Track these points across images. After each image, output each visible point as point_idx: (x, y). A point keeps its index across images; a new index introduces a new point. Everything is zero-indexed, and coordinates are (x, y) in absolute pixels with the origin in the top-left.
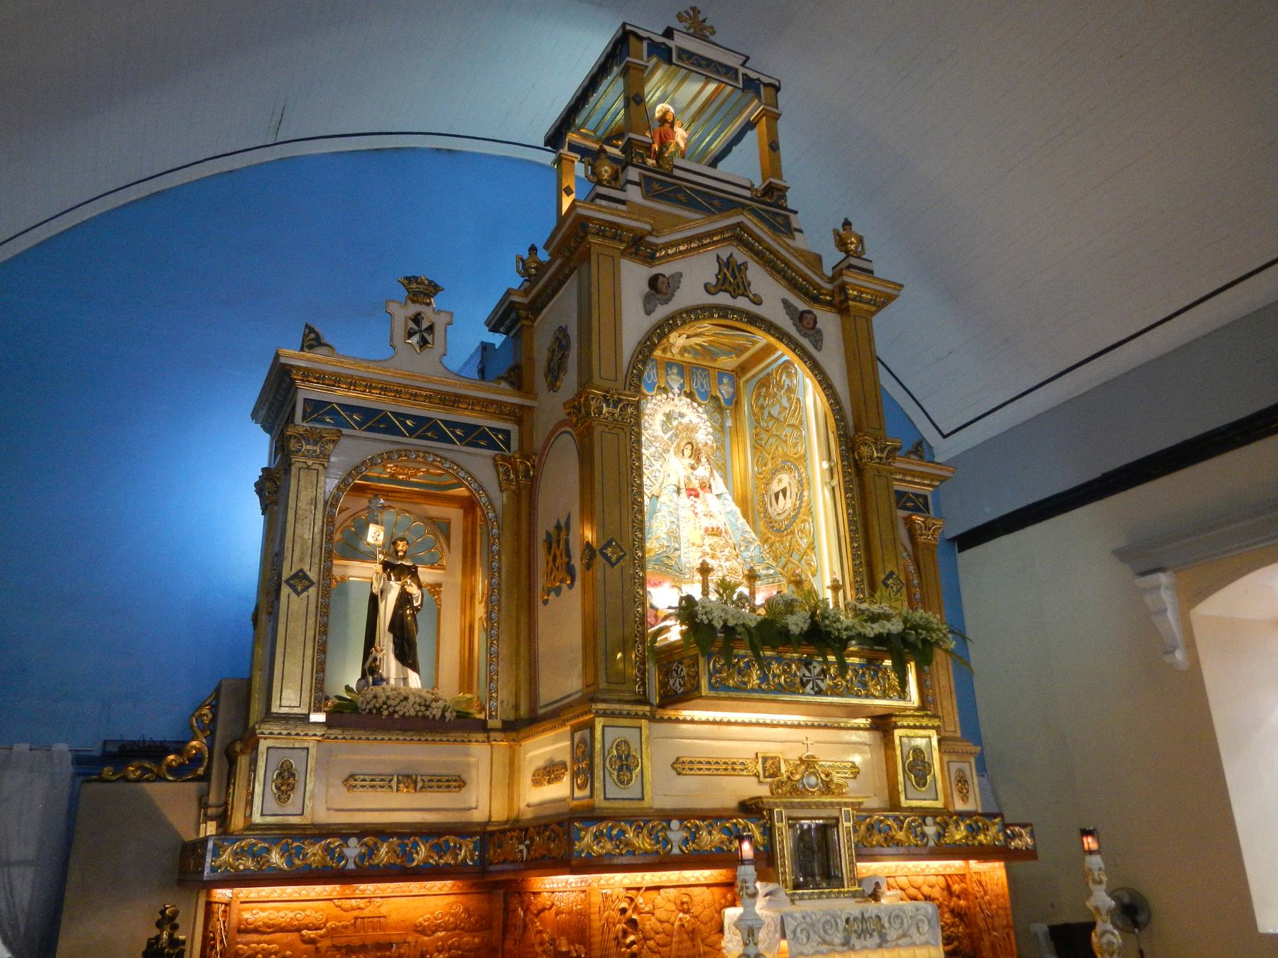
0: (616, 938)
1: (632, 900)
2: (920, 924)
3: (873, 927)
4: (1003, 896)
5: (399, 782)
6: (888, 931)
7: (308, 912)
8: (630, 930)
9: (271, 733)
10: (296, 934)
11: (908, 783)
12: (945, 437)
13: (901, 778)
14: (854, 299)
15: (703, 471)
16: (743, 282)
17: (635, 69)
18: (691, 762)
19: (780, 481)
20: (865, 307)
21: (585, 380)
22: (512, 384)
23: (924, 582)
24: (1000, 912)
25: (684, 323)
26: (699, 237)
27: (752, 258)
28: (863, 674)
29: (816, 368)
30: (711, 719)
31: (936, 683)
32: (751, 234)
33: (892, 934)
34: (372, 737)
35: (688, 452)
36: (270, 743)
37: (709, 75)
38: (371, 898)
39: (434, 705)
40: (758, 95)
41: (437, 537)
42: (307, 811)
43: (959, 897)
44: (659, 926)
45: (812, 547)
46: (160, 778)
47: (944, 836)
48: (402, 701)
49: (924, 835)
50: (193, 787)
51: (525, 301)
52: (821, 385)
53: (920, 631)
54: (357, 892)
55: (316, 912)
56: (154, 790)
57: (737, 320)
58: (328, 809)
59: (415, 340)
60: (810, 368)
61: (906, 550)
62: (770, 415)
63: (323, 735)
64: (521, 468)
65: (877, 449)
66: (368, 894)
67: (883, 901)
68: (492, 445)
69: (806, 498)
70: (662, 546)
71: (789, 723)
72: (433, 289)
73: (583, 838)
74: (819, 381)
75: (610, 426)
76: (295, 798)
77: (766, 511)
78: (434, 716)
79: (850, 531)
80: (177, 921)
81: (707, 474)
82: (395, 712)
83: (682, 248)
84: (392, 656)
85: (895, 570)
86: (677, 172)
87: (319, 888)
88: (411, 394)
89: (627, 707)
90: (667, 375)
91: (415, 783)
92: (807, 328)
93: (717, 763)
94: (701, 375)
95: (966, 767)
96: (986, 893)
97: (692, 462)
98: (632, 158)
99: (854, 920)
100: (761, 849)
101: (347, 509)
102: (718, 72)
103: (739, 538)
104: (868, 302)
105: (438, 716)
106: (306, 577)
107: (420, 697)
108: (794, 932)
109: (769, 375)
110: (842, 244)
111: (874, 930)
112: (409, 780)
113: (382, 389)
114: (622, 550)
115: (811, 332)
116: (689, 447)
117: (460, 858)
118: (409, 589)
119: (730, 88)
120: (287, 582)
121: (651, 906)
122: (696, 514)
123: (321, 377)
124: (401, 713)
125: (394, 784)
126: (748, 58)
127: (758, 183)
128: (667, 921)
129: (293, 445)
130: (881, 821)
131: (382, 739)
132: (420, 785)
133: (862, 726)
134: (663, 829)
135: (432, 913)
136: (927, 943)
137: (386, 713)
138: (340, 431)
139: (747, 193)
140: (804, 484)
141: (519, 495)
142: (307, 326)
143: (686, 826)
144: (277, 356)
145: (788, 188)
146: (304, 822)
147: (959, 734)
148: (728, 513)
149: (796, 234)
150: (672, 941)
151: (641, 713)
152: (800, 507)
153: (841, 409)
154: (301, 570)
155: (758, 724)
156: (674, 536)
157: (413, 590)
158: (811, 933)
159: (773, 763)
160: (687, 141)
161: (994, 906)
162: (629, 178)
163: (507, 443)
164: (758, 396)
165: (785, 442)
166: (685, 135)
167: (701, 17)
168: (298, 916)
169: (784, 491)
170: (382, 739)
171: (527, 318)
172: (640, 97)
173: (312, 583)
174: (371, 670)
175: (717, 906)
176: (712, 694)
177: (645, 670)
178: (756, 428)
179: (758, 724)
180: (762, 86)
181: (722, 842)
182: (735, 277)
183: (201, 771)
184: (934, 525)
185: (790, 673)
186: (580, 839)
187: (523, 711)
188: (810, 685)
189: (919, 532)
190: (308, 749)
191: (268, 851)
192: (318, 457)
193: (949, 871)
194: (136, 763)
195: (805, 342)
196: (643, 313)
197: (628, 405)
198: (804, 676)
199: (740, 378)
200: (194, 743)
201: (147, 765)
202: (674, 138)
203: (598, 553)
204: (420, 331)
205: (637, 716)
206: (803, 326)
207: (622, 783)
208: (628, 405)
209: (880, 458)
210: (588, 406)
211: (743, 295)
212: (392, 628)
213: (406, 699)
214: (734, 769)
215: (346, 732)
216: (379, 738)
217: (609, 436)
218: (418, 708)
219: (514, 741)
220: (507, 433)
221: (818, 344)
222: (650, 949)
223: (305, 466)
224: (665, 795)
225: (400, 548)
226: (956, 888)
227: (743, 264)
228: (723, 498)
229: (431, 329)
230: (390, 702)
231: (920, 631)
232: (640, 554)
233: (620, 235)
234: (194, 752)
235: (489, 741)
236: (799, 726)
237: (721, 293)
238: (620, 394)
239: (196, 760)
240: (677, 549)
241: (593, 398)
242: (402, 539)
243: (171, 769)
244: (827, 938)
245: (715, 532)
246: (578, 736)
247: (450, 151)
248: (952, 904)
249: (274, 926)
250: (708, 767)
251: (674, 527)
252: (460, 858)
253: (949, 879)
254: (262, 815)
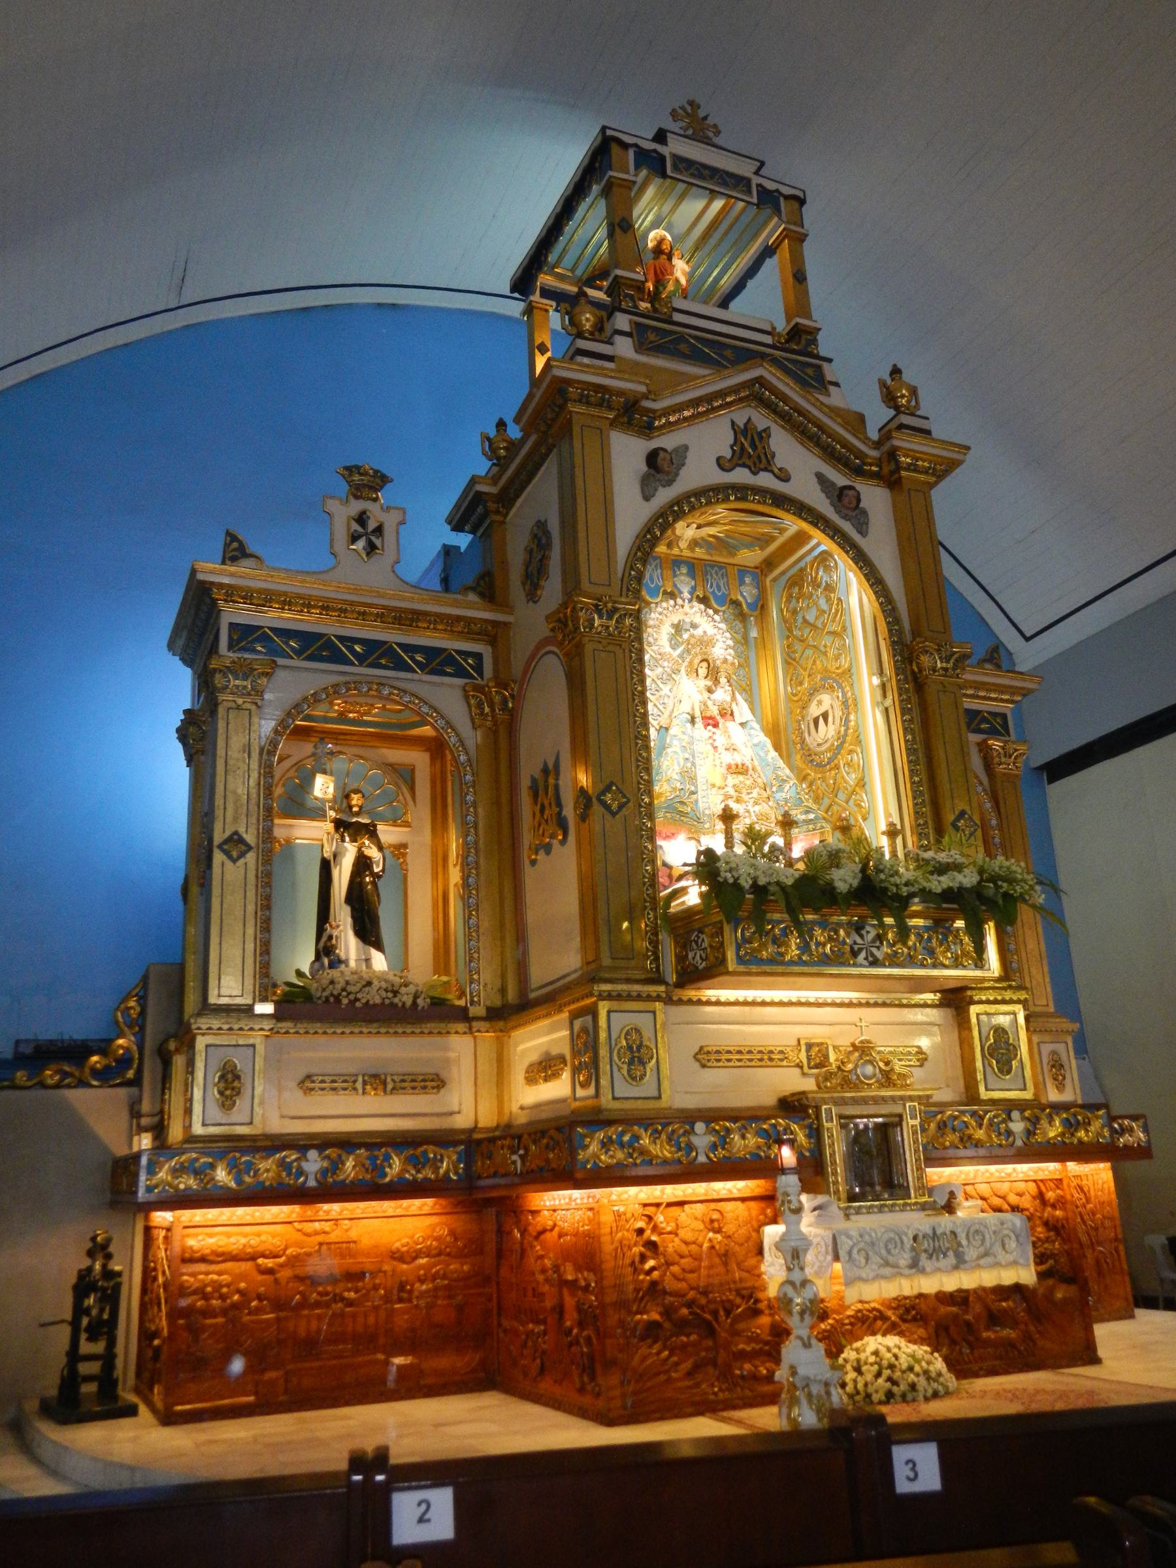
0: (633, 1263)
1: (650, 1218)
2: (1007, 1241)
3: (947, 1245)
4: (1110, 1204)
5: (365, 1083)
6: (966, 1250)
7: (263, 1238)
8: (648, 1254)
9: (210, 1029)
10: (250, 1264)
11: (988, 1069)
12: (1027, 639)
13: (979, 1064)
14: (908, 468)
15: (722, 694)
16: (765, 454)
17: (620, 186)
18: (718, 1052)
19: (820, 703)
20: (923, 477)
21: (572, 585)
22: (482, 595)
23: (1004, 821)
24: (1107, 1223)
25: (693, 508)
26: (709, 398)
27: (776, 422)
28: (930, 939)
29: (861, 559)
30: (741, 999)
31: (1022, 948)
32: (774, 391)
33: (971, 1254)
34: (330, 1031)
35: (703, 671)
36: (209, 1040)
37: (717, 189)
38: (337, 1220)
39: (403, 990)
40: (777, 211)
41: (399, 788)
42: (257, 1120)
43: (1054, 1206)
44: (684, 1249)
45: (862, 783)
46: (82, 1083)
47: (1035, 1134)
48: (364, 986)
49: (1009, 1133)
50: (122, 1092)
51: (494, 490)
52: (868, 580)
53: (1000, 883)
54: (321, 1213)
55: (273, 1237)
56: (76, 1096)
57: (759, 502)
58: (283, 1117)
59: (360, 544)
60: (852, 559)
61: (981, 783)
62: (805, 621)
63: (271, 1029)
64: (497, 699)
65: (941, 658)
66: (333, 1215)
67: (959, 1214)
68: (461, 673)
69: (852, 723)
70: (675, 789)
71: (838, 1001)
72: (380, 480)
73: (587, 1147)
74: (865, 575)
75: (604, 642)
76: (242, 1103)
77: (803, 741)
78: (404, 1003)
79: (910, 762)
80: (111, 1249)
81: (728, 699)
82: (357, 1000)
83: (686, 413)
84: (351, 934)
85: (967, 808)
86: (678, 317)
87: (275, 1209)
88: (359, 613)
89: (636, 988)
90: (675, 576)
91: (385, 1083)
92: (848, 508)
93: (750, 1052)
94: (717, 573)
95: (1061, 1048)
96: (1088, 1200)
97: (709, 683)
98: (621, 301)
99: (924, 1237)
100: (807, 1154)
101: (289, 756)
102: (725, 184)
103: (771, 776)
104: (926, 472)
105: (409, 1003)
106: (241, 841)
107: (386, 981)
108: (850, 1253)
109: (802, 570)
110: (889, 398)
111: (948, 1249)
112: (377, 1081)
113: (323, 608)
114: (624, 796)
115: (854, 514)
116: (705, 664)
117: (442, 1171)
118: (368, 852)
119: (741, 205)
120: (220, 847)
121: (673, 1224)
122: (715, 748)
123: (248, 596)
124: (364, 1001)
125: (359, 1085)
126: (762, 164)
127: (781, 326)
128: (694, 1243)
129: (219, 681)
130: (956, 1118)
131: (343, 1033)
132: (390, 1086)
133: (929, 1002)
134: (686, 1133)
135: (412, 1237)
136: (1015, 1263)
137: (345, 1001)
138: (274, 662)
139: (768, 340)
140: (849, 705)
141: (496, 732)
142: (228, 533)
143: (714, 1130)
144: (194, 572)
145: (820, 329)
146: (254, 1132)
147: (1051, 1009)
148: (755, 745)
149: (832, 388)
150: (700, 1267)
151: (654, 994)
152: (846, 735)
153: (894, 609)
154: (236, 833)
155: (799, 1004)
156: (689, 775)
157: (373, 852)
158: (871, 1253)
159: (819, 1051)
160: (690, 276)
161: (1099, 1216)
162: (617, 327)
163: (479, 669)
164: (790, 597)
165: (825, 654)
166: (687, 268)
167: (701, 114)
168: (252, 1242)
169: (825, 716)
170: (343, 1033)
171: (498, 512)
172: (627, 222)
173: (250, 848)
174: (326, 950)
175: (755, 1225)
176: (742, 968)
177: (657, 941)
178: (788, 637)
179: (799, 1004)
180: (782, 199)
181: (759, 1147)
182: (755, 448)
183: (130, 1074)
184: (1016, 750)
185: (837, 940)
186: (585, 1147)
187: (512, 996)
188: (863, 955)
189: (996, 760)
190: (253, 1046)
191: (212, 1167)
192: (249, 694)
193: (1040, 1176)
194: (54, 1066)
195: (847, 527)
196: (639, 497)
197: (625, 615)
198: (855, 943)
199: (766, 576)
200: (121, 1041)
201: (67, 1068)
202: (672, 274)
203: (594, 800)
204: (366, 534)
205: (649, 998)
206: (844, 506)
207: (634, 1079)
208: (625, 615)
209: (946, 669)
210: (576, 620)
211: (766, 470)
212: (349, 900)
213: (369, 984)
214: (771, 1059)
215: (299, 1025)
216: (339, 1031)
217: (603, 655)
218: (384, 994)
219: (501, 1031)
220: (478, 657)
221: (862, 526)
222: (674, 1276)
223: (233, 705)
224: (687, 1093)
225: (354, 802)
226: (1050, 1195)
227: (764, 430)
228: (748, 726)
229: (379, 530)
230: (349, 988)
231: (1000, 883)
232: (647, 800)
233: (609, 401)
234: (121, 1052)
235: (471, 1033)
236: (850, 1005)
237: (738, 469)
238: (615, 602)
239: (125, 1062)
240: (693, 793)
241: (582, 609)
242: (356, 791)
243: (95, 1073)
244: (891, 1259)
245: (739, 770)
246: (578, 1024)
247: (394, 306)
248: (1046, 1215)
249: (222, 1254)
250: (738, 1057)
251: (689, 765)
252: (442, 1171)
253: (1041, 1184)
254: (204, 1125)
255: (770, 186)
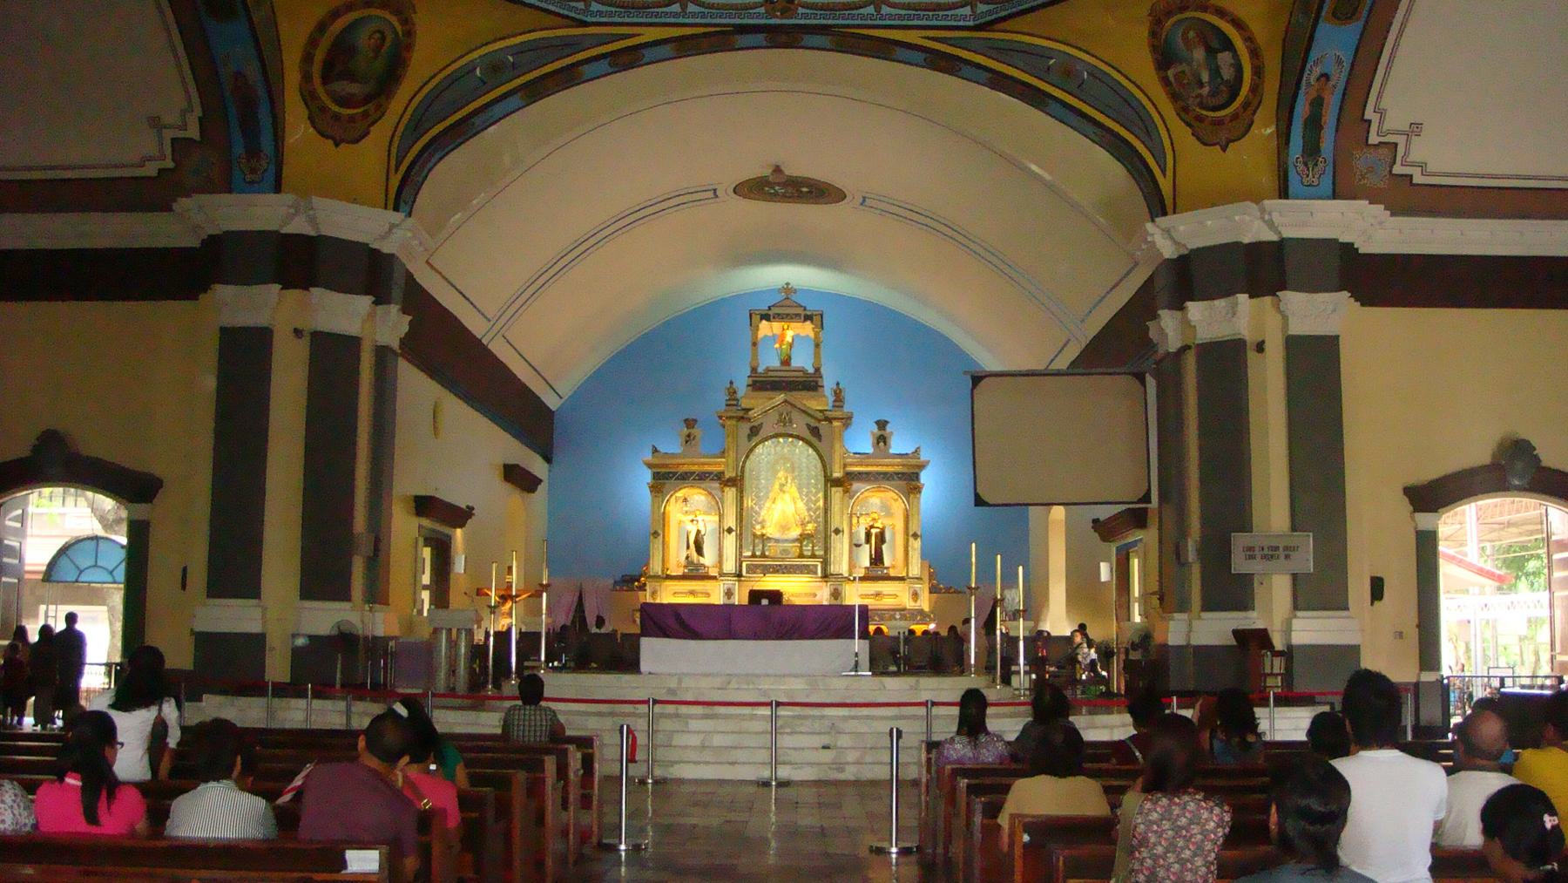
86: (770, 374)
112: (692, 593)
255: (809, 313)
